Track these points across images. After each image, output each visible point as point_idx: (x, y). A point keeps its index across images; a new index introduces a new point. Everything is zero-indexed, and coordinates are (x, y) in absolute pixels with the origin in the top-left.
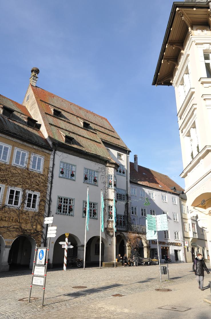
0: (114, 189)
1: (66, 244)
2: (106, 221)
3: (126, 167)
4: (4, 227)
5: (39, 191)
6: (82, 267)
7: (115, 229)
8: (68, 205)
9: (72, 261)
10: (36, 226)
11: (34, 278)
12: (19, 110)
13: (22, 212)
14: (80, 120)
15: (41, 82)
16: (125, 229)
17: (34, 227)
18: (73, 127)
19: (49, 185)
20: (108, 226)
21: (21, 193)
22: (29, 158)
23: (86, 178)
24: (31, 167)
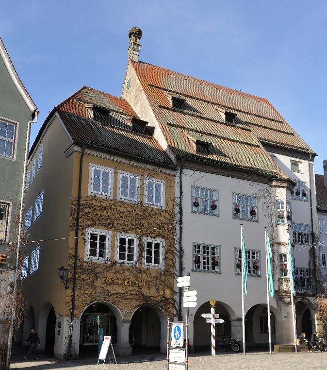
0: (288, 225)
1: (212, 317)
2: (277, 279)
3: (308, 185)
4: (117, 293)
5: (163, 237)
6: (241, 351)
7: (293, 292)
8: (210, 256)
9: (224, 342)
10: (163, 291)
11: (170, 365)
12: (117, 109)
13: (141, 271)
14: (219, 109)
15: (149, 51)
16: (311, 292)
17: (161, 292)
18: (206, 121)
19: (177, 227)
20: (281, 288)
21: (136, 243)
22: (142, 186)
23: (237, 211)
24: (146, 200)
